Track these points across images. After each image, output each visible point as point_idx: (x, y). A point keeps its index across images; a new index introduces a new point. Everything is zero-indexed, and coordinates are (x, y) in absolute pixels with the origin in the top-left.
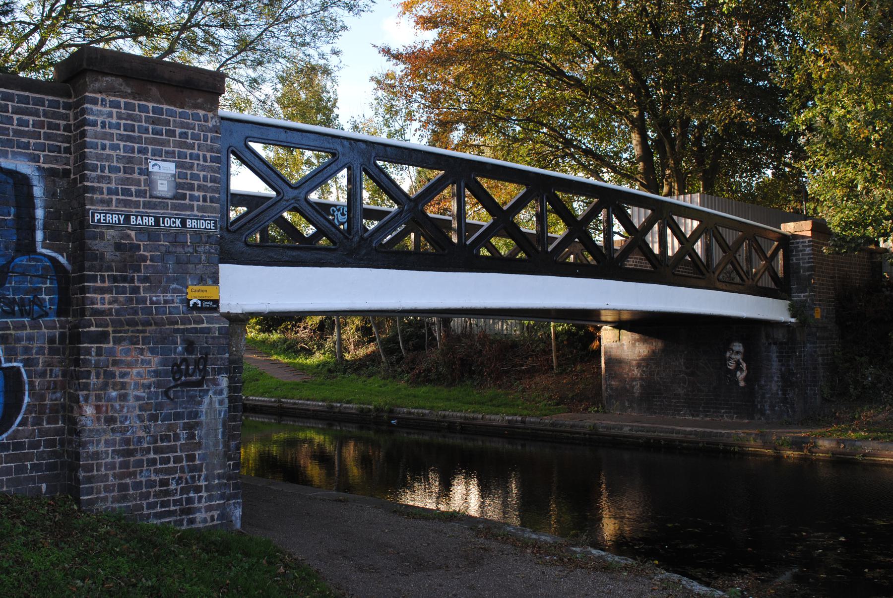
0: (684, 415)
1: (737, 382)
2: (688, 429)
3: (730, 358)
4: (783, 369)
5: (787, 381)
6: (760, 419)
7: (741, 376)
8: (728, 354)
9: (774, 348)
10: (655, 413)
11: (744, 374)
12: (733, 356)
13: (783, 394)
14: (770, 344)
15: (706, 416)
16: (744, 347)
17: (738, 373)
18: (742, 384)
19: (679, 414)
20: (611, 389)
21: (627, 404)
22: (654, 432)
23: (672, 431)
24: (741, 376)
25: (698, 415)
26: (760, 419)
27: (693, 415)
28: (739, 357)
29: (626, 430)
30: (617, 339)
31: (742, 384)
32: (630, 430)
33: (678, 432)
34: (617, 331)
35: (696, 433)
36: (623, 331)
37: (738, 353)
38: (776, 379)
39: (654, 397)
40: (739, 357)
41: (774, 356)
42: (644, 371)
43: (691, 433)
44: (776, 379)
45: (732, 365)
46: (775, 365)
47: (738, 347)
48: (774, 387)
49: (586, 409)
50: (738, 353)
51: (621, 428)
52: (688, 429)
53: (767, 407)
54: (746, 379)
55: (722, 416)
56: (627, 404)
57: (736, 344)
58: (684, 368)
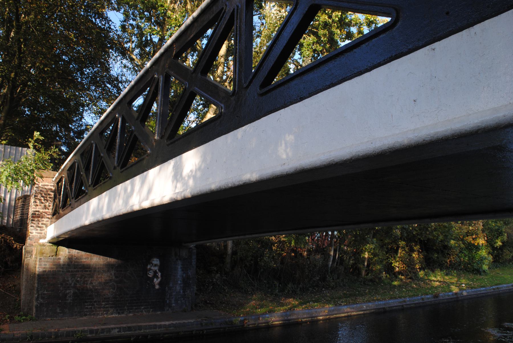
0: (112, 314)
1: (154, 286)
2: (167, 323)
3: (150, 269)
4: (184, 275)
5: (186, 283)
6: (168, 310)
7: (156, 281)
8: (149, 267)
9: (179, 262)
10: (86, 315)
11: (159, 280)
12: (152, 268)
13: (183, 292)
14: (177, 259)
15: (130, 312)
16: (160, 261)
17: (155, 280)
18: (157, 287)
19: (106, 314)
20: (43, 298)
21: (58, 310)
22: (156, 328)
23: (155, 327)
24: (156, 281)
25: (123, 313)
26: (168, 310)
27: (119, 313)
28: (156, 268)
29: (115, 332)
30: (54, 254)
31: (157, 287)
32: (118, 332)
33: (160, 326)
34: (55, 247)
35: (174, 326)
36: (61, 248)
37: (156, 265)
38: (179, 282)
39: (86, 302)
40: (156, 268)
41: (179, 267)
42: (78, 281)
43: (170, 326)
44: (179, 282)
45: (151, 274)
46: (180, 272)
47: (156, 261)
48: (178, 288)
49: (11, 319)
50: (156, 265)
51: (109, 330)
52: (167, 323)
53: (173, 302)
54: (160, 284)
55: (142, 311)
56: (58, 310)
57: (155, 259)
58: (114, 278)
